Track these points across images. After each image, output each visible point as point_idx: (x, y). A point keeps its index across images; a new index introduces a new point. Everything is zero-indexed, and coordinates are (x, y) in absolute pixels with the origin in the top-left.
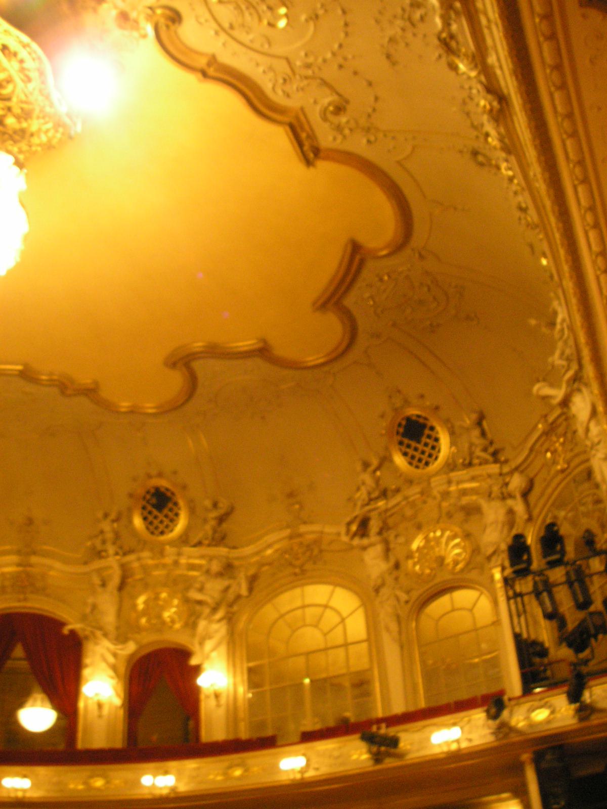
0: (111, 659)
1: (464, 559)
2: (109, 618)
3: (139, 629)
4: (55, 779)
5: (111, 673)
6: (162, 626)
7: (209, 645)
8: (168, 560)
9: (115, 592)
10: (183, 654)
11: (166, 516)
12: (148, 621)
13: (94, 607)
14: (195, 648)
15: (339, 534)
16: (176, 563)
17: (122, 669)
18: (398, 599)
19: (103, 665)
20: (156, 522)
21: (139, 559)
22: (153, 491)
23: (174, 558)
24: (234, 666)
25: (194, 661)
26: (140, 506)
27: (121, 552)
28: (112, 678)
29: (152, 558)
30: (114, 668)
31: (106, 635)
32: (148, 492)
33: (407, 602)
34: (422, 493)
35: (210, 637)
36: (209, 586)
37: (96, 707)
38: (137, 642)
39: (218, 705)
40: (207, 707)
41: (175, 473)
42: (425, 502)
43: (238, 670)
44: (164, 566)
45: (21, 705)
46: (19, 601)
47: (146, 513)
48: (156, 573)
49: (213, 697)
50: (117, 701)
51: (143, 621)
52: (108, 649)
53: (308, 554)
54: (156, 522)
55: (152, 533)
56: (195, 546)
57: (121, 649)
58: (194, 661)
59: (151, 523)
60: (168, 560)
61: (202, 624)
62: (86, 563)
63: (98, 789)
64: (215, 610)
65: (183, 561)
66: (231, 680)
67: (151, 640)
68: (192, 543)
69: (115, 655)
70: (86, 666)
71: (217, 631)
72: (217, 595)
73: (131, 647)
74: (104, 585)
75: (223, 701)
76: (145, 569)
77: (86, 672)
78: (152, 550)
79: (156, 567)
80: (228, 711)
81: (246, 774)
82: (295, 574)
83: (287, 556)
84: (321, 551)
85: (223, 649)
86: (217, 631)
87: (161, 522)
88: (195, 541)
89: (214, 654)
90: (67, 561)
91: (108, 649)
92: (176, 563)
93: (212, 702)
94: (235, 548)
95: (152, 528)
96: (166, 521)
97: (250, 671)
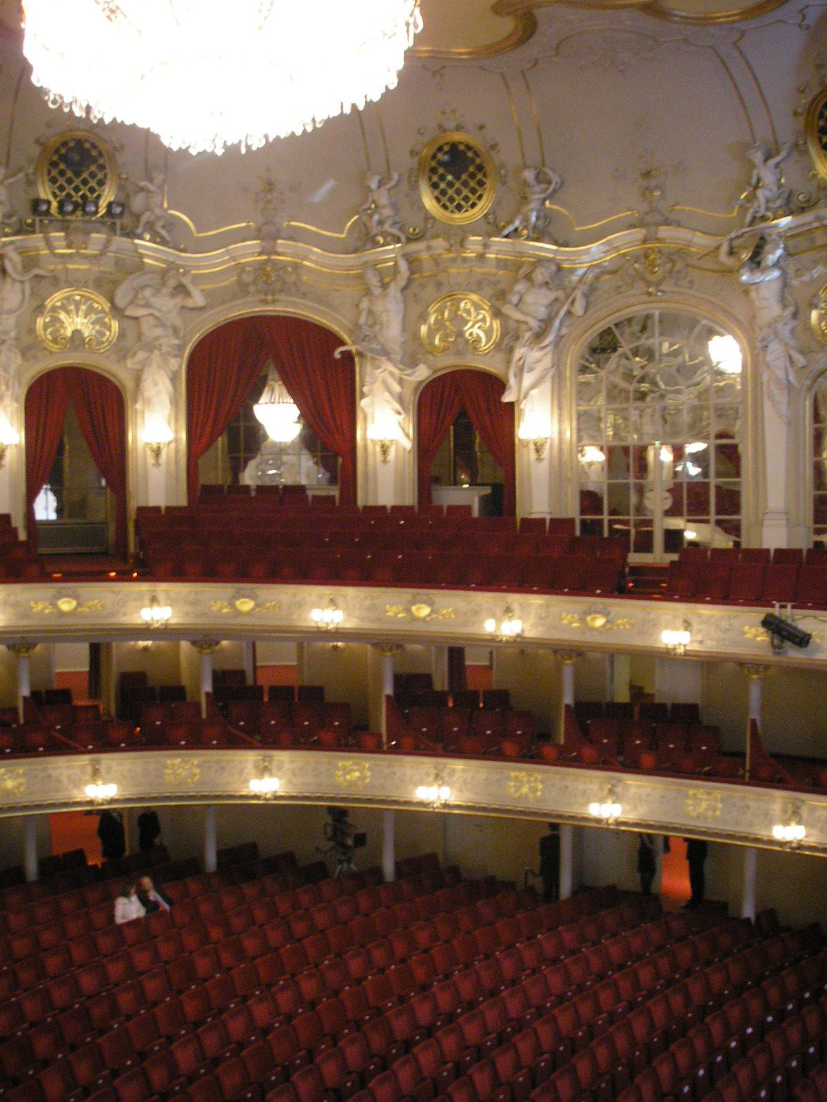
2: (393, 331)
3: (431, 350)
4: (368, 602)
5: (398, 407)
7: (528, 379)
9: (399, 295)
10: (491, 386)
11: (465, 184)
13: (370, 312)
14: (512, 381)
15: (718, 248)
16: (481, 257)
17: (411, 399)
18: (790, 358)
19: (386, 394)
20: (450, 192)
21: (429, 248)
22: (446, 148)
23: (480, 248)
25: (507, 398)
26: (428, 168)
27: (403, 239)
28: (399, 413)
29: (449, 251)
30: (400, 399)
31: (389, 360)
32: (440, 149)
33: (803, 367)
35: (531, 370)
36: (529, 299)
37: (378, 449)
38: (429, 367)
39: (539, 459)
40: (525, 459)
41: (481, 127)
43: (566, 415)
44: (465, 260)
45: (256, 398)
46: (265, 302)
47: (435, 179)
48: (453, 270)
49: (532, 447)
50: (408, 444)
52: (391, 373)
53: (669, 266)
54: (450, 192)
55: (445, 207)
56: (506, 237)
57: (406, 375)
58: (507, 398)
59: (443, 193)
61: (517, 354)
62: (356, 251)
64: (539, 336)
66: (556, 428)
67: (449, 362)
68: (506, 232)
69: (401, 382)
70: (363, 395)
71: (538, 361)
72: (542, 312)
73: (422, 373)
74: (384, 286)
75: (545, 454)
76: (436, 261)
77: (363, 404)
78: (447, 238)
79: (454, 260)
80: (551, 465)
81: (609, 626)
82: (650, 294)
83: (637, 266)
85: (547, 386)
86: (538, 361)
87: (458, 192)
88: (510, 228)
89: (534, 392)
90: (328, 246)
91: (391, 373)
93: (533, 456)
95: (444, 200)
96: (465, 192)
97: (579, 416)
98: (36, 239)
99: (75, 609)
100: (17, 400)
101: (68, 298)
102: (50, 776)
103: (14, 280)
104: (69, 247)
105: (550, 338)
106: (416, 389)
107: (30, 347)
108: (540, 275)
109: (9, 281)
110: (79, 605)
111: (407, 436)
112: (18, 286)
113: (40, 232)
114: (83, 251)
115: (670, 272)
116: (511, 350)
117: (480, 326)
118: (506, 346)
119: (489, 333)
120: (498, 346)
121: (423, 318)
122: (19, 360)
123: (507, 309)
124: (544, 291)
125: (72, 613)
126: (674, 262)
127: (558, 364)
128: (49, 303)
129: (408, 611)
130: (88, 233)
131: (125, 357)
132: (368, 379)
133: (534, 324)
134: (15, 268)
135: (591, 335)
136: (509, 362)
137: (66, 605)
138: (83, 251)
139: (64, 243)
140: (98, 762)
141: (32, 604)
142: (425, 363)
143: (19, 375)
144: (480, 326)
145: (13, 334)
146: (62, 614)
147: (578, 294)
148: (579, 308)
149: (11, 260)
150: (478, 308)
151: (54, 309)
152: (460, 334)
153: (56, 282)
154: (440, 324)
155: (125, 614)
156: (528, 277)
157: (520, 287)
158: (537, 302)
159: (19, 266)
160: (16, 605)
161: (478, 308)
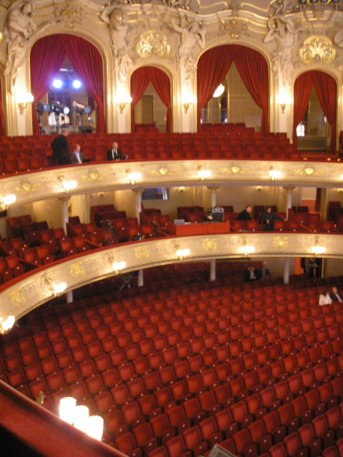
98: (301, 14)
99: (313, 173)
100: (291, 85)
101: (314, 40)
102: (297, 242)
103: (290, 33)
104: (315, 17)
107: (296, 62)
109: (288, 34)
110: (315, 171)
112: (292, 36)
113: (302, 11)
114: (321, 19)
122: (292, 67)
125: (312, 175)
128: (305, 43)
130: (323, 11)
131: (338, 66)
134: (291, 27)
137: (309, 171)
138: (321, 19)
139: (312, 16)
140: (318, 238)
141: (295, 170)
143: (292, 75)
145: (290, 57)
146: (307, 175)
149: (289, 24)
151: (307, 45)
153: (308, 33)
155: (333, 176)
159: (293, 27)
160: (288, 170)
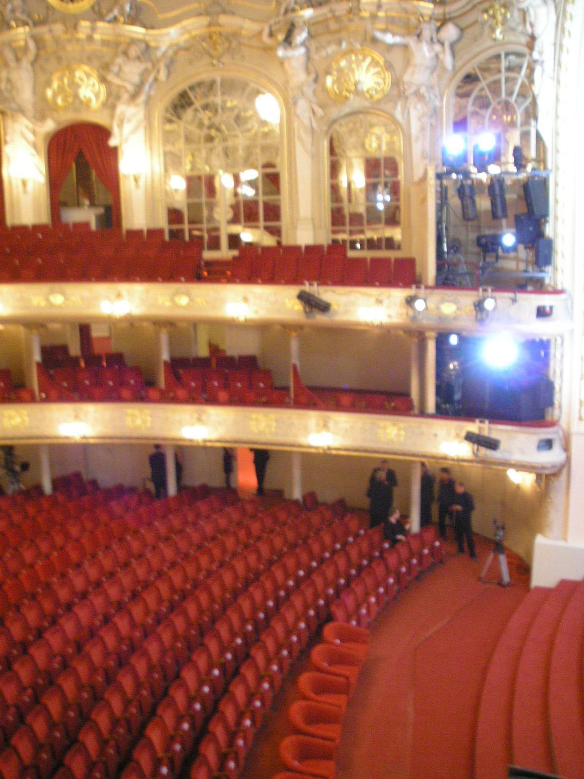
0: (31, 137)
1: (383, 90)
3: (55, 108)
5: (33, 151)
6: (80, 104)
7: (127, 128)
8: (82, 35)
9: (29, 67)
10: (101, 133)
12: (65, 100)
13: (9, 81)
14: (115, 130)
15: (260, 33)
16: (90, 38)
17: (43, 147)
18: (314, 113)
19: (24, 142)
21: (51, 31)
24: (151, 148)
25: (112, 142)
27: (31, 23)
30: (35, 146)
33: (322, 118)
34: (350, 11)
35: (129, 121)
39: (137, 186)
42: (351, 20)
44: (78, 40)
48: (70, 48)
51: (60, 101)
52: (27, 127)
53: (226, 45)
58: (112, 142)
60: (82, 35)
61: (121, 108)
63: (60, 307)
64: (134, 96)
65: (97, 37)
67: (69, 117)
69: (34, 133)
72: (136, 79)
73: (50, 126)
74: (18, 60)
75: (142, 182)
76: (57, 41)
83: (204, 44)
84: (240, 44)
85: (141, 133)
88: (110, 16)
92: (90, 38)
94: (152, 28)
97: (165, 154)
105: (142, 98)
106: (45, 138)
108: (134, 51)
111: (40, 172)
115: (228, 49)
116: (113, 108)
117: (90, 89)
118: (110, 105)
119: (97, 95)
120: (105, 105)
121: (49, 84)
123: (111, 77)
124: (137, 64)
126: (230, 42)
127: (148, 117)
129: (47, 300)
132: (9, 131)
133: (130, 88)
135: (174, 94)
136: (112, 116)
142: (53, 119)
144: (90, 89)
147: (162, 67)
148: (162, 76)
150: (88, 76)
152: (76, 96)
154: (61, 89)
156: (125, 53)
157: (120, 60)
158: (132, 71)
161: (88, 76)
